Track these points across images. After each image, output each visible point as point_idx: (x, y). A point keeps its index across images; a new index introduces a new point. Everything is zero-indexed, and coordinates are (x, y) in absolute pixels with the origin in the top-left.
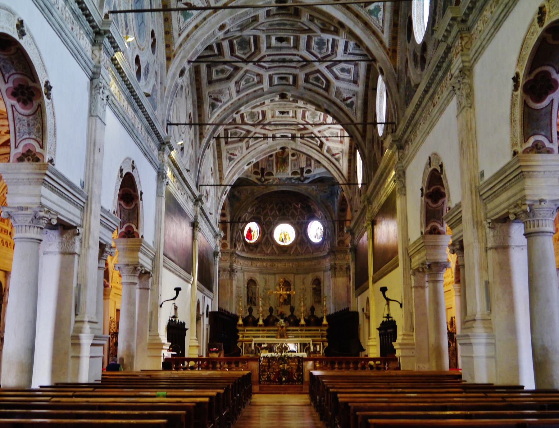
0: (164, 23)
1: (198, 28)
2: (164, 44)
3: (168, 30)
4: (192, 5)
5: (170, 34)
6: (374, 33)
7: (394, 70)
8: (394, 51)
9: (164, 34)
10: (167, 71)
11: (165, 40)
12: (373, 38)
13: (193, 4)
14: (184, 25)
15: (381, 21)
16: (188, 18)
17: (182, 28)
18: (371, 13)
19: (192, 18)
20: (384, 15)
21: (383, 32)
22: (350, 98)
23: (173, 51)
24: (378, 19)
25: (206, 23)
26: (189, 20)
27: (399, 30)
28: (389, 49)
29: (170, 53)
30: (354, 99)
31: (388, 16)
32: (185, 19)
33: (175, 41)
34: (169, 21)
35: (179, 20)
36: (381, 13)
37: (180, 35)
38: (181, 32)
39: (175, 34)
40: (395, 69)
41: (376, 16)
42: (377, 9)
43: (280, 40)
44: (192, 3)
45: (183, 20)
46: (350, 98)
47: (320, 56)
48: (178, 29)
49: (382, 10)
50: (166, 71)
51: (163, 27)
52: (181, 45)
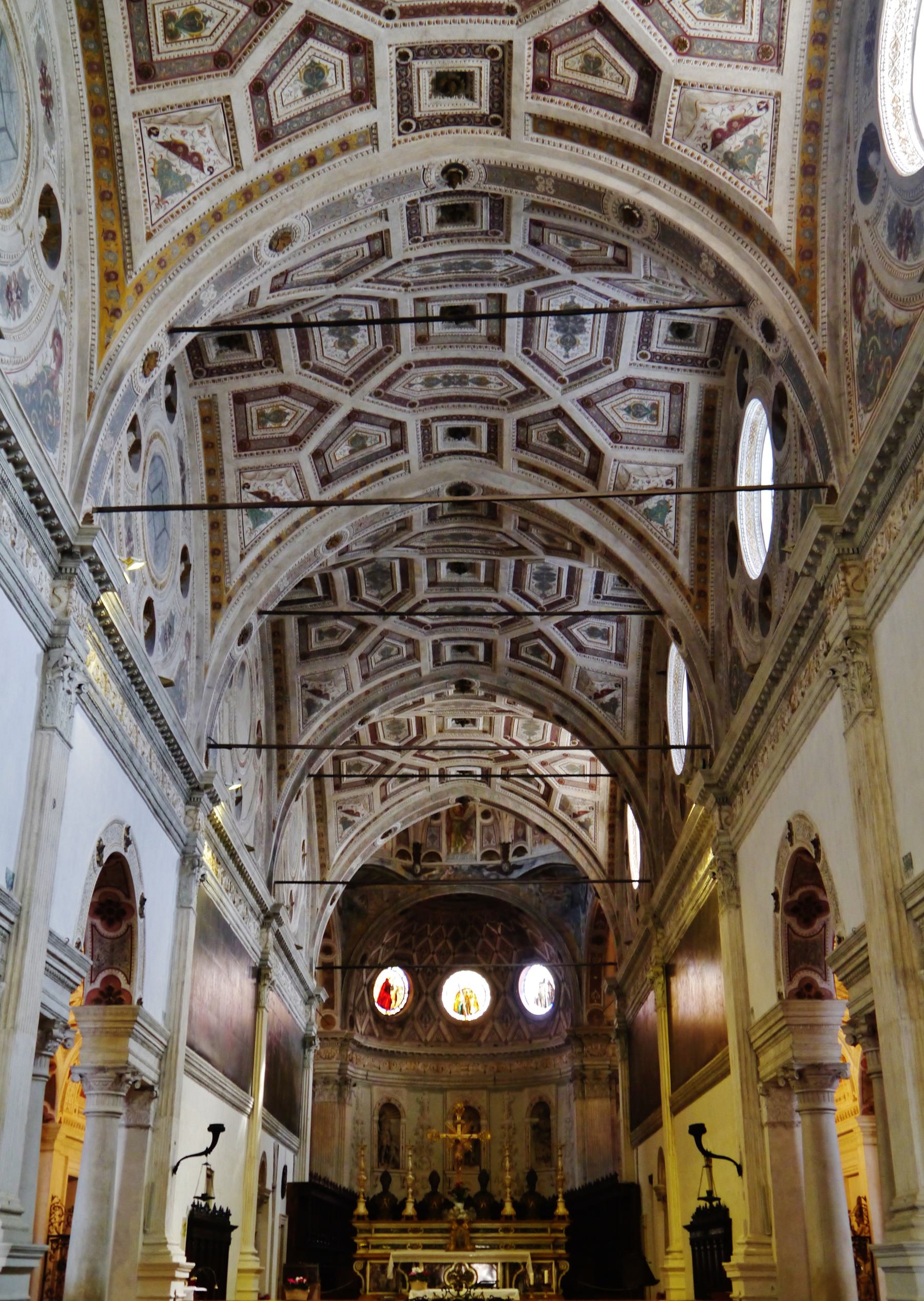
0: (210, 533)
1: (283, 543)
2: (208, 576)
3: (219, 547)
6: (658, 555)
7: (702, 634)
8: (703, 594)
9: (208, 554)
10: (213, 632)
11: (211, 567)
12: (656, 566)
15: (672, 532)
16: (261, 523)
17: (247, 542)
18: (649, 514)
20: (677, 519)
21: (676, 554)
22: (609, 691)
23: (227, 589)
24: (664, 527)
26: (262, 526)
27: (711, 550)
28: (692, 590)
29: (221, 595)
30: (618, 693)
31: (686, 521)
32: (255, 527)
33: (232, 569)
34: (221, 527)
35: (241, 526)
36: (672, 515)
37: (242, 557)
40: (706, 632)
41: (662, 522)
42: (664, 508)
43: (457, 568)
44: (271, 492)
46: (609, 691)
47: (542, 602)
49: (673, 509)
50: (209, 631)
51: (207, 540)
52: (243, 579)
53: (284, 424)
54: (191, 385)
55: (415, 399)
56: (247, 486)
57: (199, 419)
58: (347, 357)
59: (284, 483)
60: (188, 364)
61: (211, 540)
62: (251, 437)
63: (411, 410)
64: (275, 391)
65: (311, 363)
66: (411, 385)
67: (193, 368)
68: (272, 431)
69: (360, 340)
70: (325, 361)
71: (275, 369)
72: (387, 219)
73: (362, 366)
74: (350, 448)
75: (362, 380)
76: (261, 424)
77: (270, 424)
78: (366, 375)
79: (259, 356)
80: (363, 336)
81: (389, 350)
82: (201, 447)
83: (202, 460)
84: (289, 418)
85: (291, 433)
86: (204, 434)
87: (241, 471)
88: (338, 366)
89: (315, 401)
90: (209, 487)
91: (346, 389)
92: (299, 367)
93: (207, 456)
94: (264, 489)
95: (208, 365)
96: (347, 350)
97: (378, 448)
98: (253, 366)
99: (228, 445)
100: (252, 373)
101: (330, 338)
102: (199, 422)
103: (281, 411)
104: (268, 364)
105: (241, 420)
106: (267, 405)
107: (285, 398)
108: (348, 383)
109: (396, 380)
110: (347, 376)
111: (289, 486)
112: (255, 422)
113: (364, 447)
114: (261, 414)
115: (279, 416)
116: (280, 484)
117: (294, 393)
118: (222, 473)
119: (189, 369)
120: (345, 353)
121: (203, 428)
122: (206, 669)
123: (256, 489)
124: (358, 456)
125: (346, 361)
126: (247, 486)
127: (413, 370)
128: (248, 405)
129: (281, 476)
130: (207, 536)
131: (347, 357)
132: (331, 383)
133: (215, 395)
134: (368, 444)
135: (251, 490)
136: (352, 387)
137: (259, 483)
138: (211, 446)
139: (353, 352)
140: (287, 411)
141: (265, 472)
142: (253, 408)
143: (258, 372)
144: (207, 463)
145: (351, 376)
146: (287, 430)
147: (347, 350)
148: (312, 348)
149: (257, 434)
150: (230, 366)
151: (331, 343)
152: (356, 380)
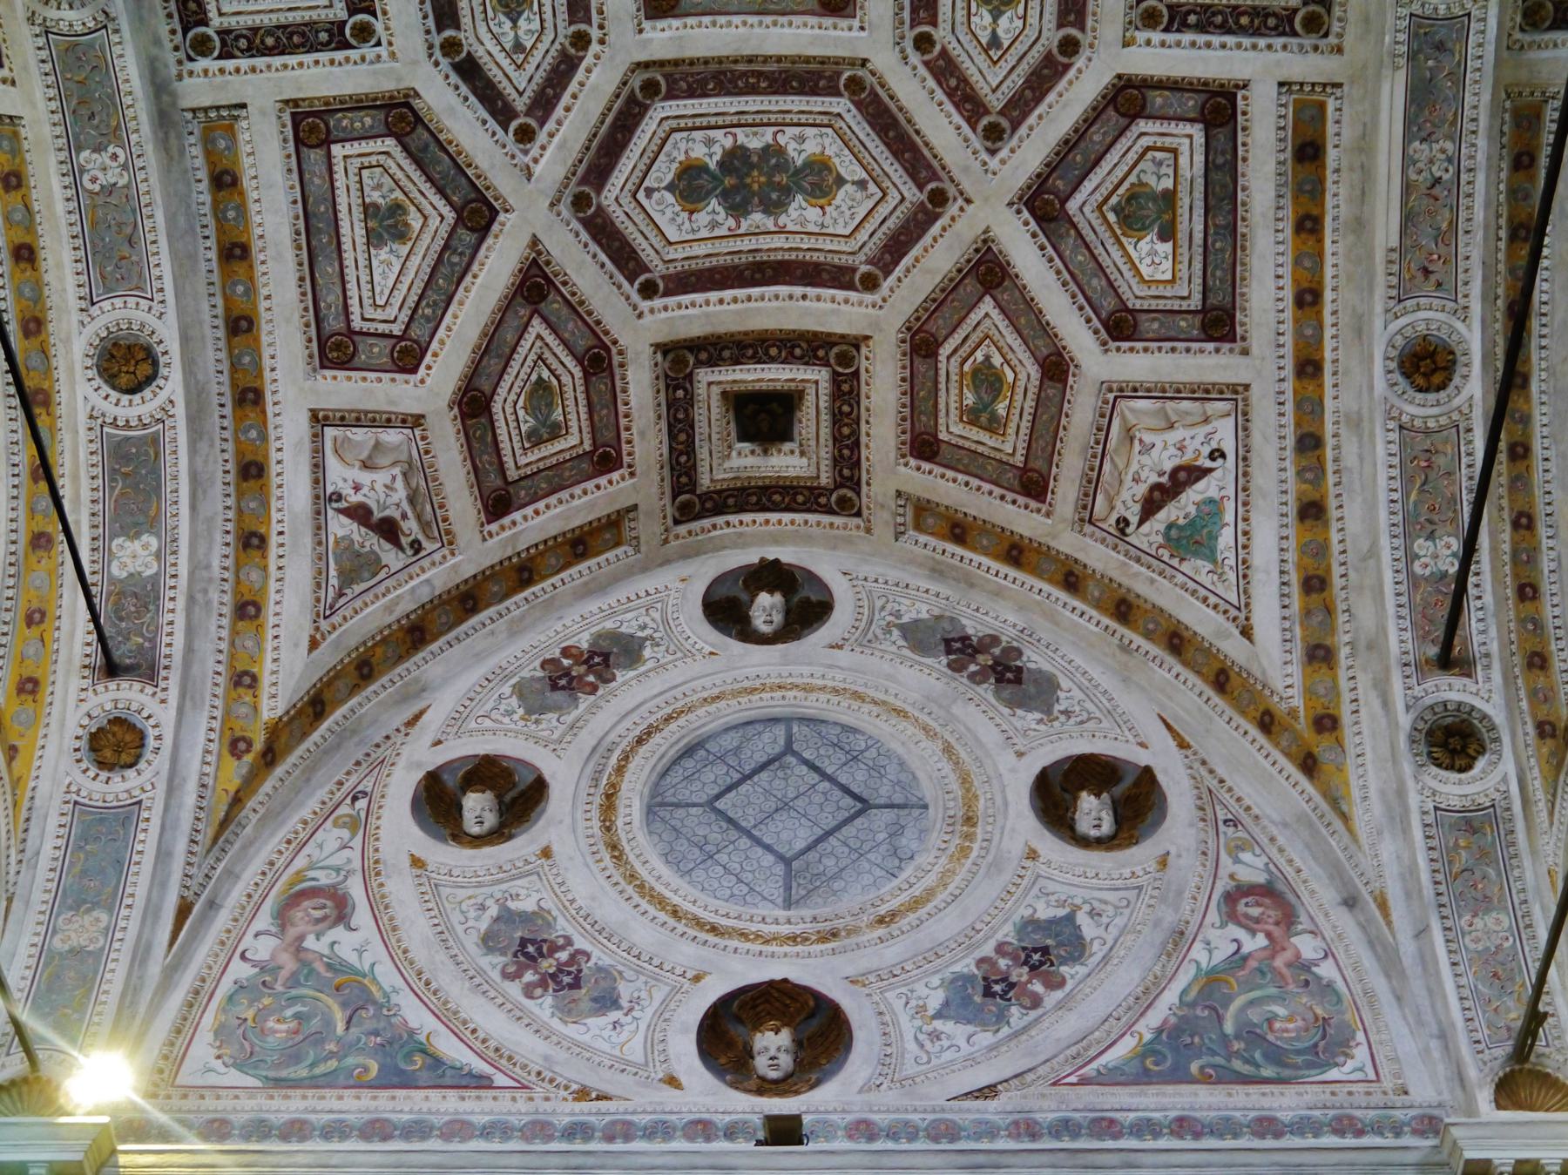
0: (1186, 664)
2: (1254, 732)
3: (1216, 666)
4: (1164, 480)
5: (1232, 674)
9: (1216, 699)
10: (1345, 818)
11: (1243, 713)
13: (1161, 474)
14: (1232, 576)
16: (1214, 537)
17: (1233, 599)
19: (1229, 517)
23: (1293, 713)
25: (1337, 447)
26: (1226, 538)
29: (1297, 737)
32: (1211, 557)
34: (1185, 634)
35: (1194, 589)
37: (1246, 632)
38: (1242, 616)
39: (1233, 648)
44: (1154, 479)
45: (1210, 567)
48: (1221, 618)
50: (1338, 824)
51: (1193, 679)
52: (1320, 655)
53: (1010, 376)
54: (868, 530)
55: (1052, 37)
56: (1123, 523)
57: (951, 548)
58: (861, 184)
59: (1148, 438)
60: (812, 518)
61: (1198, 673)
62: (1019, 460)
63: (1085, 53)
64: (922, 366)
65: (864, 268)
66: (995, 41)
67: (831, 512)
68: (1016, 406)
69: (811, 148)
70: (863, 236)
71: (864, 350)
72: (243, 106)
73: (897, 154)
74: (1152, 236)
75: (935, 163)
76: (994, 425)
77: (1001, 408)
78: (926, 152)
79: (821, 375)
80: (801, 139)
81: (855, 85)
82: (1013, 572)
83: (1039, 584)
84: (997, 360)
85: (1034, 371)
86: (986, 552)
87: (1086, 518)
88: (883, 210)
89: (971, 285)
90: (1098, 606)
91: (953, 209)
92: (868, 297)
93: (1036, 572)
94: (1141, 490)
95: (825, 479)
96: (840, 181)
97: (1192, 163)
98: (846, 394)
99: (1020, 519)
100: (864, 402)
101: (793, 210)
102: (959, 550)
103: (976, 372)
104: (845, 359)
105: (970, 463)
106: (953, 398)
107: (945, 351)
108: (939, 198)
109: (964, 80)
110: (913, 194)
111: (1171, 427)
112: (984, 436)
113: (1169, 199)
114: (972, 416)
115: (987, 380)
116: (1147, 449)
117: (938, 326)
118: (1076, 561)
119: (826, 519)
120: (848, 187)
121: (974, 549)
122: (1383, 906)
123: (1137, 508)
124: (1190, 219)
125: (872, 187)
126: (1123, 523)
127: (941, 34)
128: (943, 436)
129: (1129, 436)
130: (1186, 673)
131: (861, 184)
132: (927, 239)
133: (899, 494)
134: (1168, 183)
135: (1134, 520)
136: (952, 191)
137: (1126, 495)
138: (1016, 552)
139: (848, 167)
140: (979, 356)
141: (1107, 467)
142: (952, 428)
143: (864, 388)
144: (1050, 581)
145: (921, 187)
146: (1022, 376)
147: (840, 181)
148: (816, 257)
149: (1011, 445)
150: (837, 439)
151: (813, 214)
152: (937, 178)
